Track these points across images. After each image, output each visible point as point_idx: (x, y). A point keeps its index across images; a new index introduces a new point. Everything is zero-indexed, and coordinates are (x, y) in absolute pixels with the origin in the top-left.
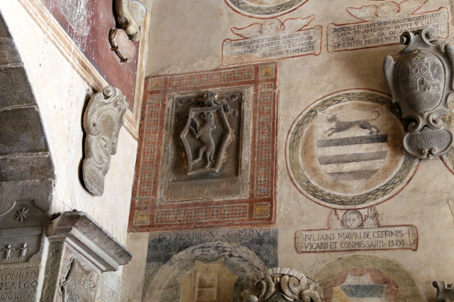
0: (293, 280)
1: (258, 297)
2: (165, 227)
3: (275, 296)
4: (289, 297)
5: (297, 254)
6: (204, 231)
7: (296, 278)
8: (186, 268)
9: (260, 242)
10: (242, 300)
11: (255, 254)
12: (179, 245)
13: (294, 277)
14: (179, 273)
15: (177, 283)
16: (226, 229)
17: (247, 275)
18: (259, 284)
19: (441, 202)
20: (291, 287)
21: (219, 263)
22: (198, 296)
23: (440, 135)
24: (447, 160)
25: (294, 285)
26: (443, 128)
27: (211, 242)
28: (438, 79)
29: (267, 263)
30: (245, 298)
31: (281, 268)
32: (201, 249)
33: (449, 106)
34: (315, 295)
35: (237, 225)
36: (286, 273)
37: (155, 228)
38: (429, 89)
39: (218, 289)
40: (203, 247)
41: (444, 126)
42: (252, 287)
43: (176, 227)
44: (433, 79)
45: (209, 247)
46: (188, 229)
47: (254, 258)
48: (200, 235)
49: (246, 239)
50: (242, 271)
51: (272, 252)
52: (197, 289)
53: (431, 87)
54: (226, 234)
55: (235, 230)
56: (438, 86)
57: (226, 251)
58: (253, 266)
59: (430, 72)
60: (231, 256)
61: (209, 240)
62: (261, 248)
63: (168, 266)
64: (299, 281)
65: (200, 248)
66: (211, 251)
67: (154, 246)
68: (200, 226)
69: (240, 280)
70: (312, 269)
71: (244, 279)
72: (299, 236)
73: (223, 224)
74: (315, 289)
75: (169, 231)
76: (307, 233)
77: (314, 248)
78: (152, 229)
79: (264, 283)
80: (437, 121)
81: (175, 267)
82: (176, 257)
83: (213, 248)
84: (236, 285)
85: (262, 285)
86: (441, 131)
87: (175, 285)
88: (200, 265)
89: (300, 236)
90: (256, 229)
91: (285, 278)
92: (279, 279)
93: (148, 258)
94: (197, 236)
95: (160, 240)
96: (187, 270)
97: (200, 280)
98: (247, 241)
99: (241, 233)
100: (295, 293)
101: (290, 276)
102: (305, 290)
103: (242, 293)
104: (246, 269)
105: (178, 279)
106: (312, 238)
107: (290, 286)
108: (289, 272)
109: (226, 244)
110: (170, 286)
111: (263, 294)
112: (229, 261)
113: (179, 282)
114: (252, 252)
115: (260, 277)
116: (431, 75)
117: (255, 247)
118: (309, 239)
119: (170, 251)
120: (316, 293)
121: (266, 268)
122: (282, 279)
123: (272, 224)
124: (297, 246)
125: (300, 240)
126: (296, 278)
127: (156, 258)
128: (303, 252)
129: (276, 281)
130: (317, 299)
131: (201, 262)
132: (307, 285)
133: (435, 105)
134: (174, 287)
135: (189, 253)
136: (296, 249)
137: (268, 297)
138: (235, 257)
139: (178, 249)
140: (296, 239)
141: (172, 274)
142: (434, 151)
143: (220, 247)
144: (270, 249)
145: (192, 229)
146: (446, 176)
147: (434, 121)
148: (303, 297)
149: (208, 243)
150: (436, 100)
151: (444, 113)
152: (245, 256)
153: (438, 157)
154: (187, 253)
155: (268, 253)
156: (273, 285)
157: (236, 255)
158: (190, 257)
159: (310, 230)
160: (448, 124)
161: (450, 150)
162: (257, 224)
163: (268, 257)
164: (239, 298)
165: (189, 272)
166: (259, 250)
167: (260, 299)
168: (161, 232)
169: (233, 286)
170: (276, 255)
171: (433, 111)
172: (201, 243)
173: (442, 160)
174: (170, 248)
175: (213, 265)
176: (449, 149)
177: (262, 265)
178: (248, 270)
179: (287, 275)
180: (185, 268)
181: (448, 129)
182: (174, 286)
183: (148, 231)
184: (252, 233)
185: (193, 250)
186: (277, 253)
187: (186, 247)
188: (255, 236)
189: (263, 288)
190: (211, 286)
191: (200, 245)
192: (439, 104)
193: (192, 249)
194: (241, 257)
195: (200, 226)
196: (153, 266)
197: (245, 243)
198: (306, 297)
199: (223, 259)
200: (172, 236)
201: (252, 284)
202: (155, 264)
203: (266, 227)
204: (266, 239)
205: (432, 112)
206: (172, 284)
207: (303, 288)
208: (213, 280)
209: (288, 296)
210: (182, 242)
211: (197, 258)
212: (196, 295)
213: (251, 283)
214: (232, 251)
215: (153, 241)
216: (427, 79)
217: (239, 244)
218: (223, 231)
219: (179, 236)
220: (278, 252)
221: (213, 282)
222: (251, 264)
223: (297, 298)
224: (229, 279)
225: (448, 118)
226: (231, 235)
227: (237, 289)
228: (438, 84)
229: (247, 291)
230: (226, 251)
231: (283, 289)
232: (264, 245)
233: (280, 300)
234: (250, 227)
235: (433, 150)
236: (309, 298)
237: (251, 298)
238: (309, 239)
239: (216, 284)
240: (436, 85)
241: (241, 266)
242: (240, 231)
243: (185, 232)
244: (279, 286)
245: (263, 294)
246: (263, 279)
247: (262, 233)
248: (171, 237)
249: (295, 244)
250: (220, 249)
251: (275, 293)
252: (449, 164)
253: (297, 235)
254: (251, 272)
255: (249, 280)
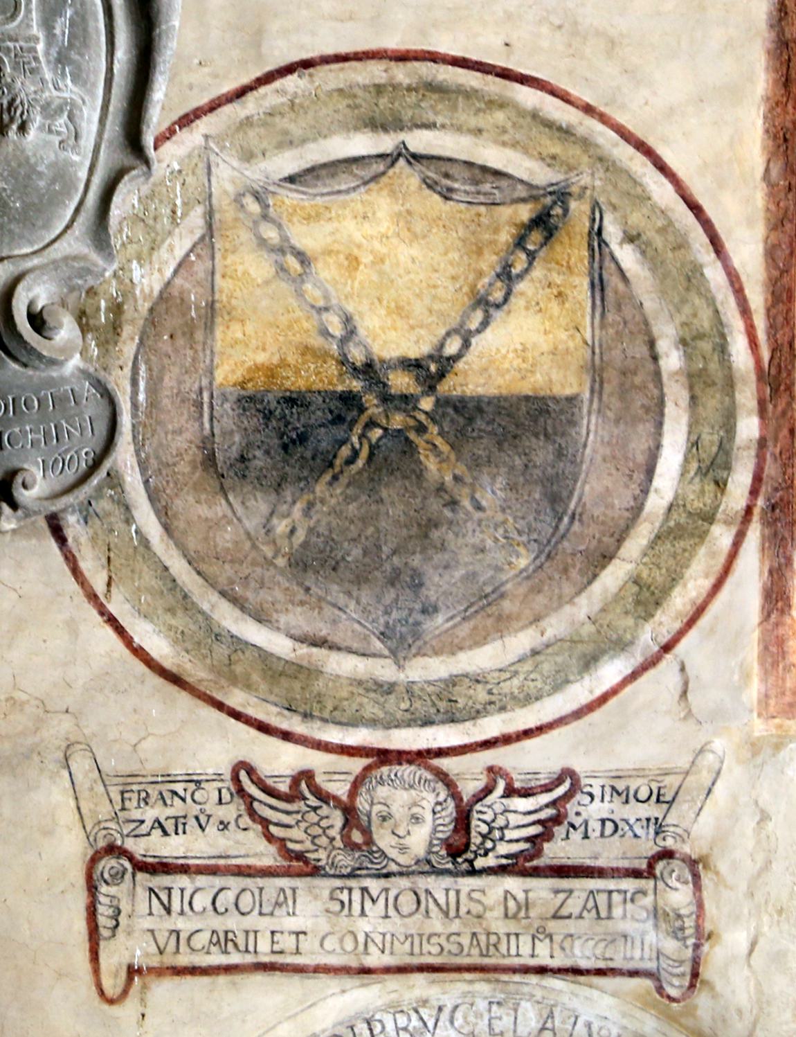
19: (36, 758)
23: (59, 401)
24: (83, 540)
26: (75, 362)
28: (76, 78)
33: (116, 242)
38: (23, 128)
41: (84, 352)
44: (48, 75)
53: (37, 120)
56: (71, 117)
59: (36, 30)
80: (50, 321)
86: (63, 380)
116: (40, 47)
133: (47, 226)
142: (25, 486)
146: (72, 627)
147: (38, 321)
150: (53, 200)
151: (91, 281)
153: (43, 524)
160: (103, 344)
161: (99, 489)
171: (36, 261)
173: (61, 539)
176: (95, 481)
181: (102, 375)
192: (68, 227)
205: (29, 264)
216: (15, 66)
225: (108, 309)
228: (73, 104)
235: (19, 479)
240: (60, 110)
252: (90, 564)
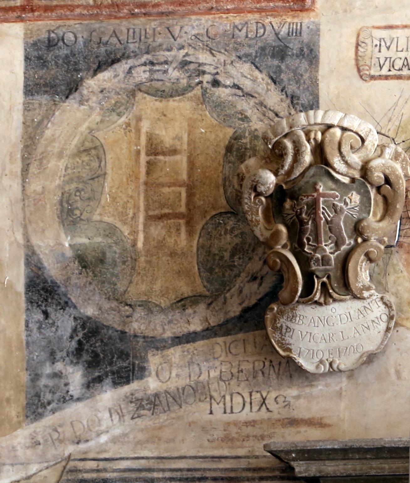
0: (350, 137)
1: (276, 174)
2: (60, 12)
3: (312, 171)
4: (342, 174)
5: (361, 82)
6: (153, 24)
7: (357, 133)
8: (115, 109)
9: (281, 52)
10: (242, 179)
11: (270, 81)
12: (97, 57)
13: (352, 131)
14: (102, 121)
15: (98, 144)
16: (203, 21)
17: (253, 129)
18: (278, 145)
20: (345, 153)
21: (190, 99)
22: (148, 173)
25: (352, 148)
27: (169, 50)
29: (295, 102)
30: (247, 176)
31: (326, 112)
32: (148, 68)
34: (394, 171)
35: (228, 11)
36: (336, 123)
37: (36, 14)
39: (189, 158)
40: (152, 63)
42: (262, 154)
43: (85, 12)
45: (166, 62)
46: (116, 18)
47: (268, 90)
48: (143, 33)
49: (250, 46)
50: (242, 119)
51: (306, 76)
52: (143, 158)
54: (203, 32)
55: (224, 23)
57: (204, 73)
58: (265, 107)
60: (216, 83)
61: (164, 47)
62: (283, 67)
63: (76, 106)
64: (363, 140)
65: (145, 64)
66: (170, 71)
67: (39, 58)
68: (143, 11)
69: (236, 137)
70: (390, 115)
71: (245, 137)
72: (366, 41)
73: (196, 9)
74: (396, 156)
75: (72, 22)
76: (384, 34)
77: (397, 67)
78: (30, 15)
79: (289, 145)
81: (91, 108)
82: (92, 84)
83: (174, 65)
84: (229, 149)
85: (285, 148)
87: (95, 148)
88: (148, 105)
89: (368, 41)
90: (271, 23)
91: (334, 134)
92: (319, 136)
93: (26, 86)
94: (137, 35)
95: (51, 44)
96: (119, 115)
97: (150, 138)
98: (252, 51)
99: (237, 31)
100: (354, 165)
101: (344, 129)
102: (374, 159)
103: (243, 167)
104: (249, 113)
105: (100, 135)
106: (393, 47)
107: (342, 150)
108: (342, 119)
109: (204, 57)
110: (83, 151)
111: (286, 168)
112: (212, 95)
113: (102, 141)
114: (264, 76)
115: (279, 131)
117: (269, 63)
118: (388, 48)
119: (77, 71)
120: (398, 166)
121: (293, 112)
122: (327, 135)
123: (307, 10)
124: (361, 63)
125: (367, 50)
126: (357, 133)
127: (46, 85)
128: (373, 78)
129: (315, 139)
130: (398, 177)
131: (148, 97)
132: (379, 149)
134: (93, 152)
135: (122, 75)
136: (359, 70)
137: (297, 173)
138: (226, 87)
139: (95, 66)
140: (360, 48)
141: (86, 124)
143: (191, 62)
144: (302, 70)
145: (124, 18)
148: (369, 173)
149: (162, 53)
152: (247, 85)
154: (116, 76)
155: (297, 78)
156: (307, 148)
157: (228, 83)
158: (123, 86)
159: (391, 27)
162: (273, 9)
163: (299, 88)
164: (236, 178)
165: (123, 119)
166: (279, 71)
167: (280, 177)
168: (52, 24)
169: (223, 152)
170: (315, 83)
172: (147, 53)
174: (76, 63)
175: (176, 104)
177: (284, 105)
178: (255, 116)
179: (338, 126)
180: (113, 110)
182: (91, 149)
183: (20, 19)
184: (262, 31)
185: (130, 68)
186: (317, 80)
187: (113, 62)
188: (270, 38)
189: (286, 154)
190: (174, 152)
191: (145, 58)
193: (128, 66)
194: (239, 88)
195: (143, 11)
196: (40, 105)
197: (247, 55)
198: (376, 174)
199: (198, 91)
200: (79, 35)
201: (262, 147)
202: (44, 99)
203: (294, 17)
204: (294, 46)
206: (88, 145)
207: (371, 155)
208: (178, 138)
209: (338, 173)
210: (103, 49)
211: (139, 87)
212: (143, 170)
213: (260, 145)
214: (217, 73)
215: (35, 44)
217: (234, 58)
218: (195, 25)
219: (94, 34)
220: (319, 78)
221: (177, 143)
222: (261, 104)
223: (357, 175)
224: (213, 136)
226: (215, 35)
227: (232, 159)
229: (251, 162)
230: (204, 73)
231: (329, 157)
232: (288, 60)
233: (321, 181)
234: (257, 16)
236: (383, 176)
237: (260, 177)
238: (388, 48)
239: (185, 147)
241: (239, 108)
242: (236, 27)
243: (110, 25)
244: (319, 151)
245: (286, 168)
246: (286, 136)
247: (284, 31)
248: (76, 38)
249: (357, 60)
250: (192, 67)
251: (311, 165)
253: (361, 38)
254: (261, 121)
255: (256, 137)
